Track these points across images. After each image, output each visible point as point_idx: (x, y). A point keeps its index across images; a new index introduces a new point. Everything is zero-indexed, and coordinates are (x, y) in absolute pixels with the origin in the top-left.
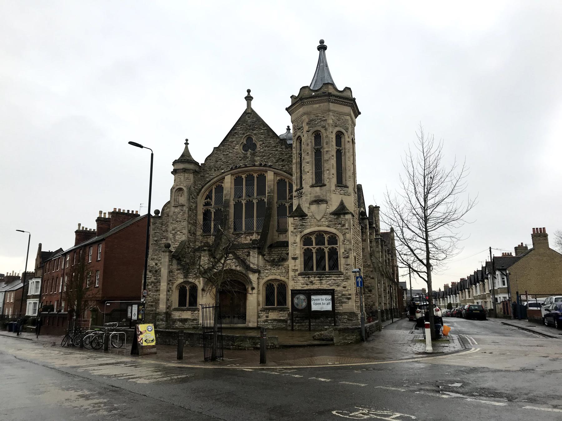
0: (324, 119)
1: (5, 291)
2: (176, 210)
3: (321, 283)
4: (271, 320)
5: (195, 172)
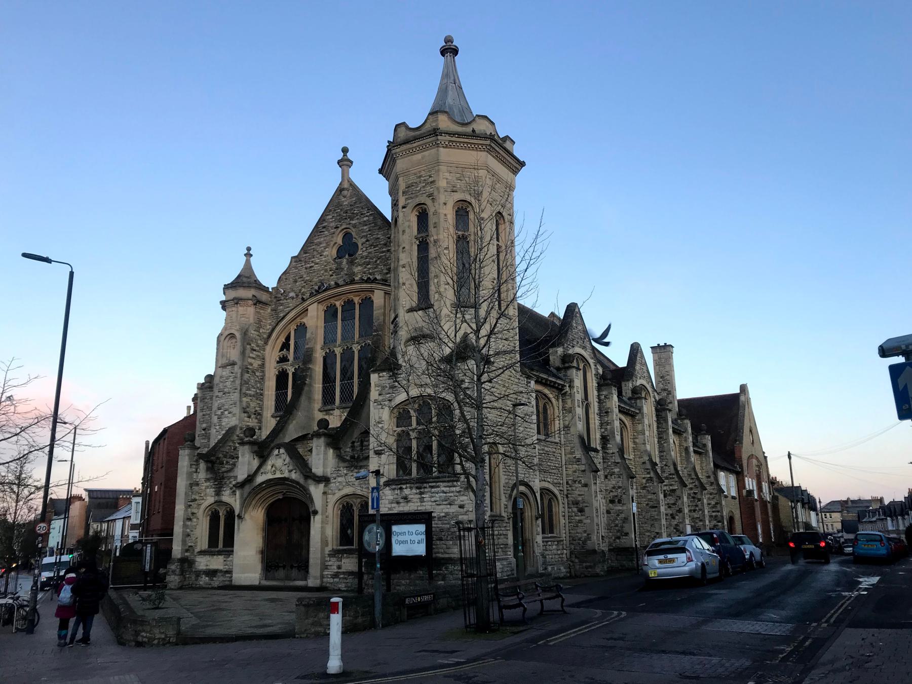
0: (431, 179)
1: (124, 518)
3: (422, 500)
4: (344, 573)
5: (257, 302)
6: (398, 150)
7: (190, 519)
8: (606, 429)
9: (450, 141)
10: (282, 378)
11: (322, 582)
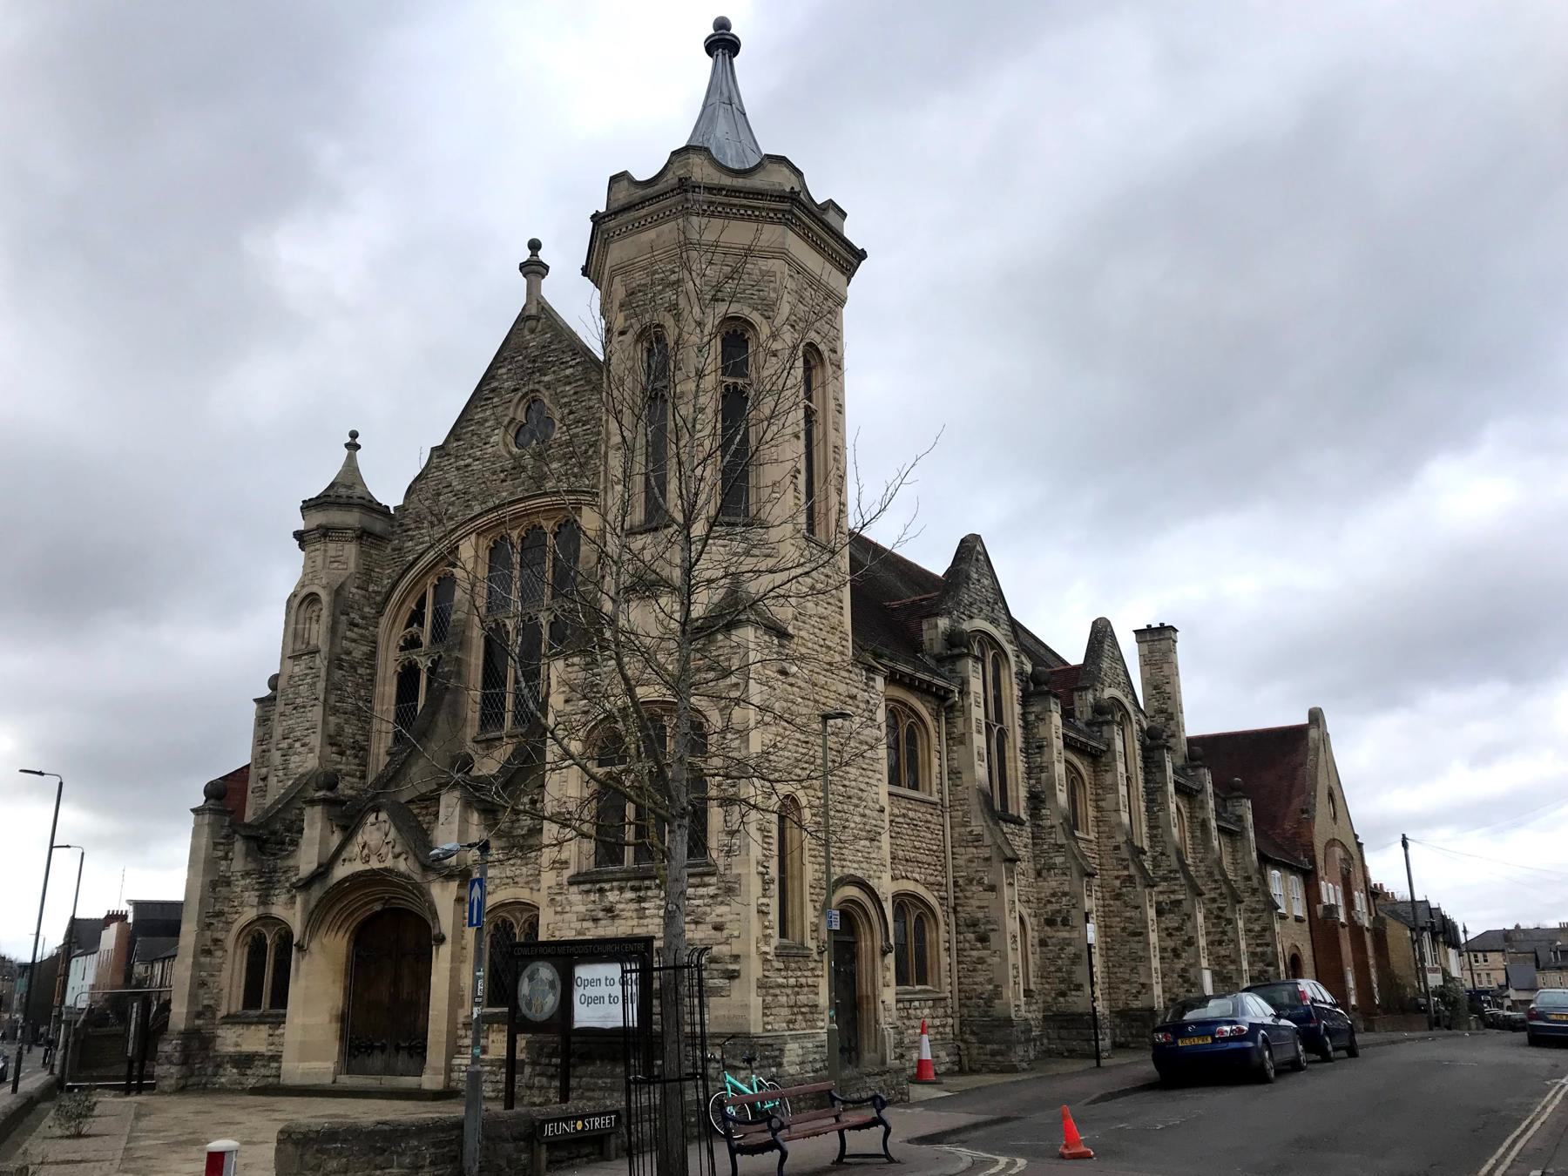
0: (674, 277)
2: (297, 669)
5: (363, 535)
6: (612, 224)
7: (208, 953)
8: (1039, 780)
9: (711, 203)
10: (408, 678)
11: (448, 1078)
